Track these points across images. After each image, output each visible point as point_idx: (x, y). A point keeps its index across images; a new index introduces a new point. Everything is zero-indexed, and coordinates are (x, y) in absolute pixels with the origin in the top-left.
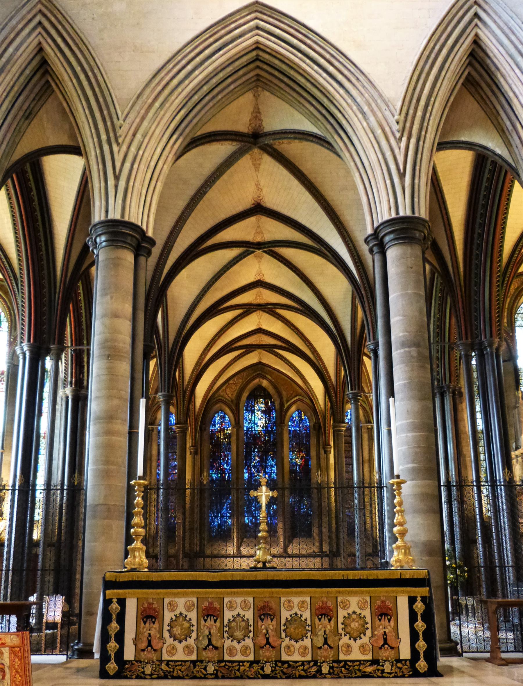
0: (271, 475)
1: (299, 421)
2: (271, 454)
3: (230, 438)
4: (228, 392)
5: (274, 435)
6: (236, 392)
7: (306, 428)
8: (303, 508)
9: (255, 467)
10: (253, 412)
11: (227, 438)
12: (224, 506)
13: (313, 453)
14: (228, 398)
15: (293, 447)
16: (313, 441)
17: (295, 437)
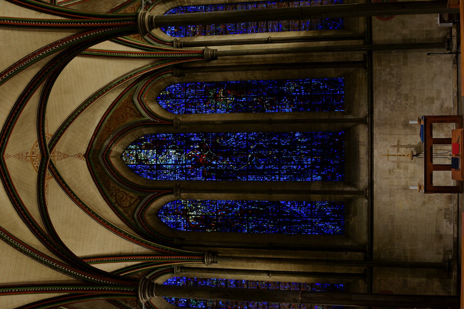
0: (250, 141)
1: (172, 99)
2: (220, 141)
3: (196, 201)
4: (128, 205)
5: (193, 136)
6: (127, 192)
7: (184, 86)
8: (300, 92)
9: (238, 165)
10: (159, 167)
11: (196, 206)
12: (295, 212)
13: (218, 77)
14: (136, 204)
15: (210, 108)
16: (201, 77)
17: (195, 105)
